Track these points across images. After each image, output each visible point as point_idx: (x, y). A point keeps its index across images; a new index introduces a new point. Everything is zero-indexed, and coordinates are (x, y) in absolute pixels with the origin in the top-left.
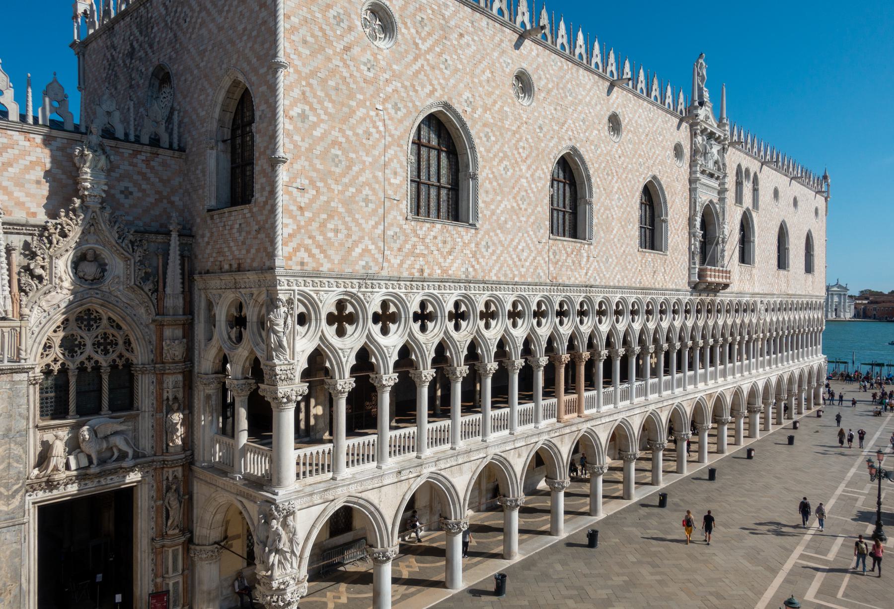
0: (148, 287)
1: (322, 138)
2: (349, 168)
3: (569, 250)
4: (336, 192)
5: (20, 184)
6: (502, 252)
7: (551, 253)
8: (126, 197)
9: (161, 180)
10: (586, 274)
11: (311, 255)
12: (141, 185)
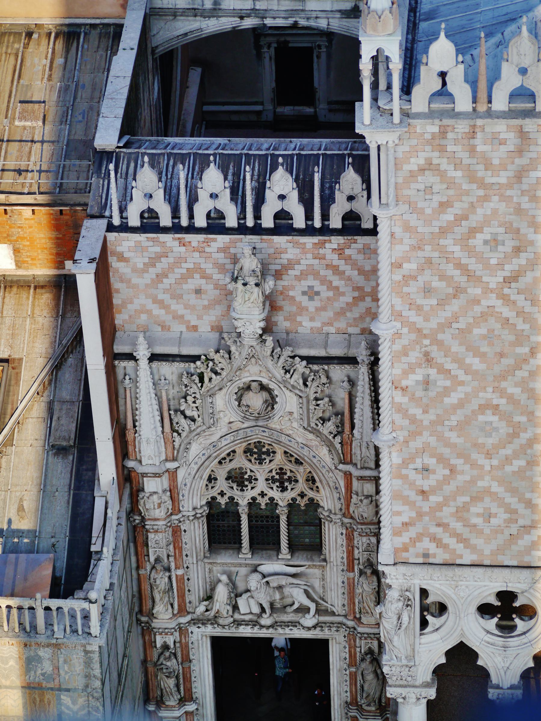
1: (461, 404)
2: (515, 435)
5: (177, 297)
8: (311, 299)
9: (361, 271)
12: (331, 282)
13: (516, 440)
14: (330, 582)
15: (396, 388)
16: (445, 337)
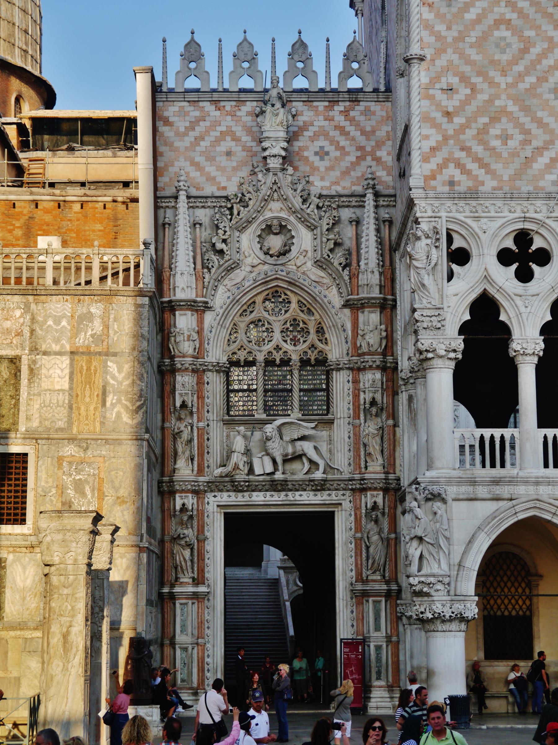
0: (338, 258)
1: (479, 20)
2: (525, 51)
4: (503, 86)
5: (211, 159)
8: (322, 159)
9: (363, 132)
12: (338, 142)
13: (527, 56)
14: (337, 441)
15: (424, 4)
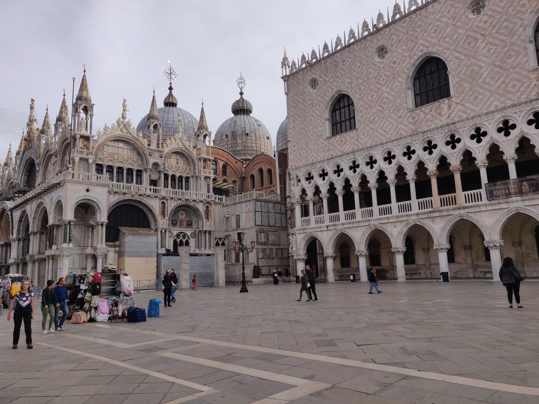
3: (427, 111)
6: (373, 133)
7: (410, 120)
10: (449, 117)
11: (298, 163)
16: (296, 116)
